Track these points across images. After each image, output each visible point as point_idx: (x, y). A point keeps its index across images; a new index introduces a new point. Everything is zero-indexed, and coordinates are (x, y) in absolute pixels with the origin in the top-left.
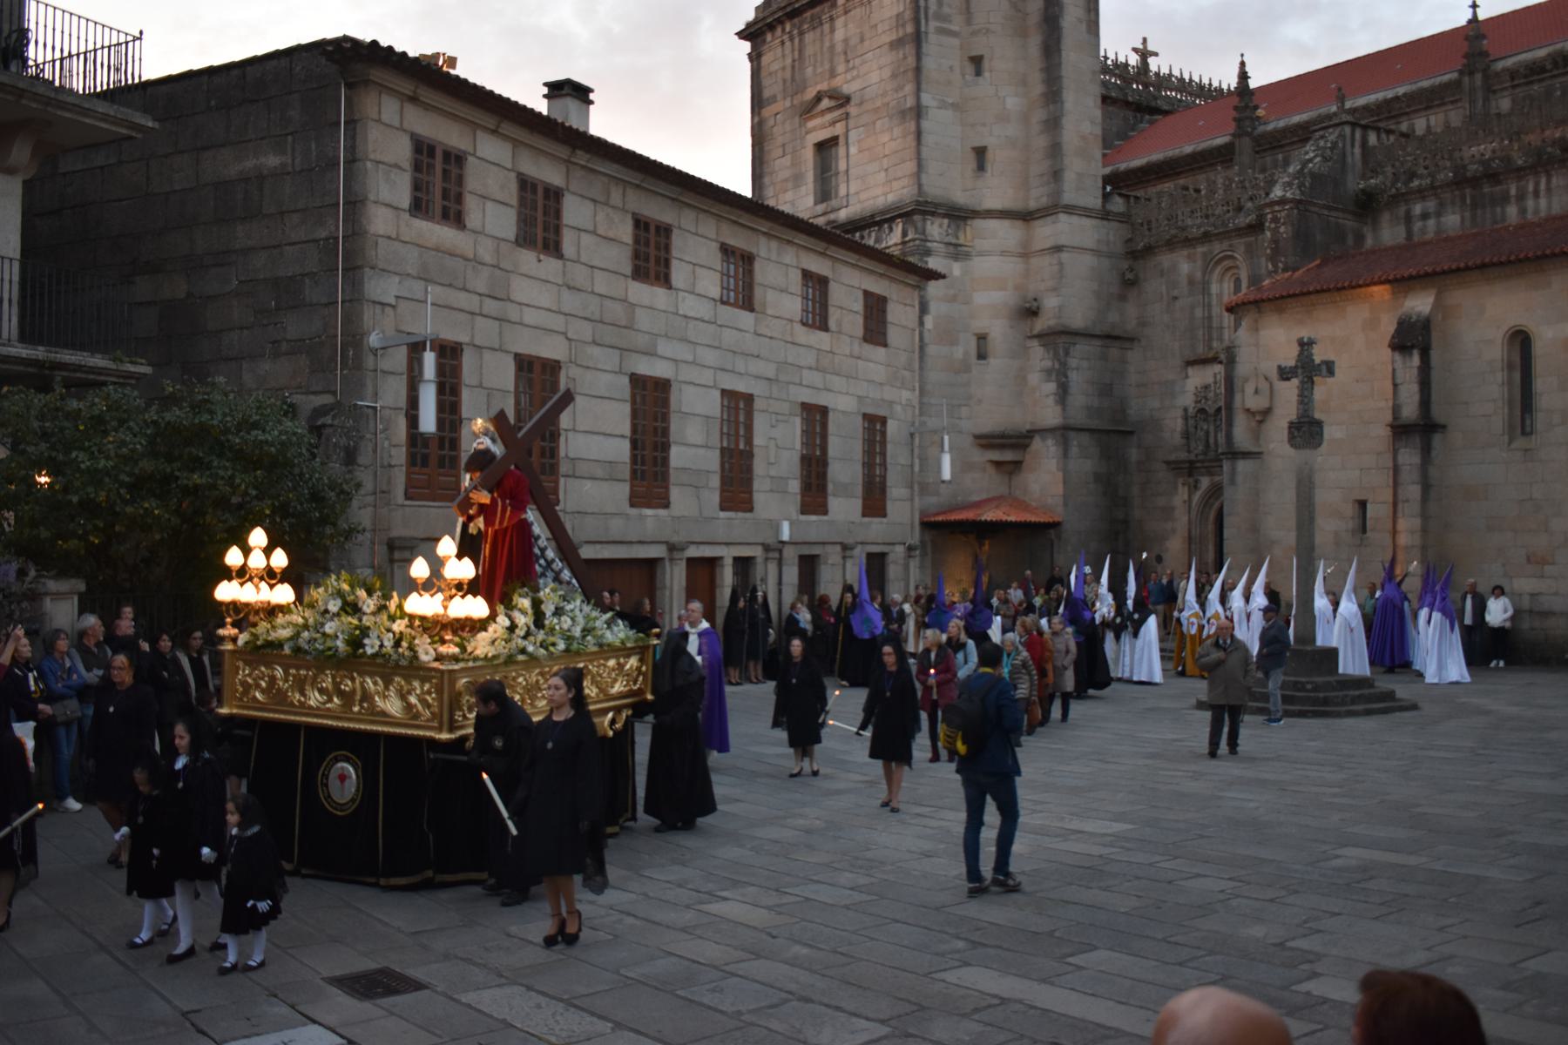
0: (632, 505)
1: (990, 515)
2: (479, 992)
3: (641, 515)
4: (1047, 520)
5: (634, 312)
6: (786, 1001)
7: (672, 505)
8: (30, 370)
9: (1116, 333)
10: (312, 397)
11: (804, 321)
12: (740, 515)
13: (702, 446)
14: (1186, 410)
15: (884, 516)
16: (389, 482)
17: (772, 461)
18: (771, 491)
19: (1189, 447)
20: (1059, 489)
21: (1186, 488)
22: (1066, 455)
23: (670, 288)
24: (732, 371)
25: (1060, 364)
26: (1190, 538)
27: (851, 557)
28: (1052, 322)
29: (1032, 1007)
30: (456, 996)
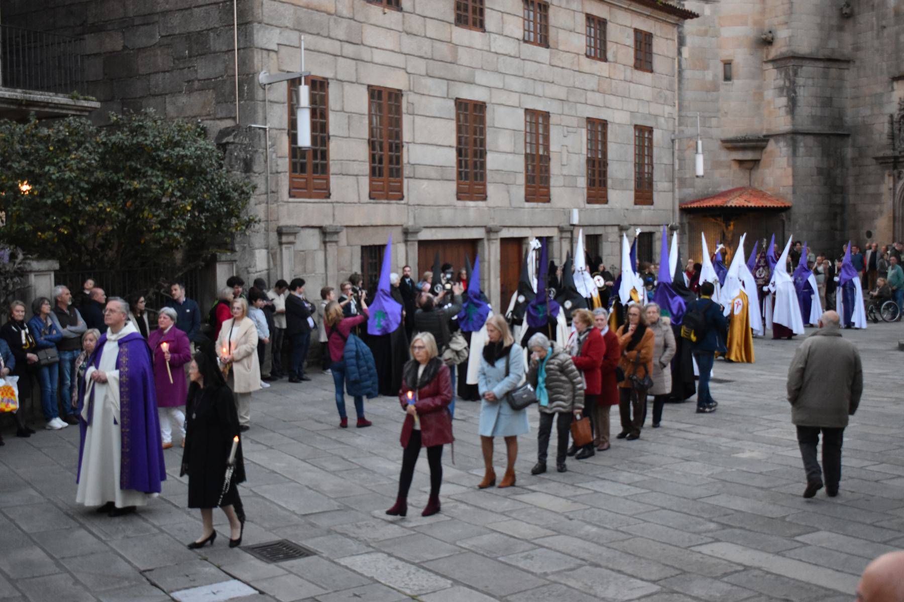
0: (459, 199)
2: (354, 557)
3: (465, 206)
4: (779, 205)
5: (456, 52)
6: (580, 566)
7: (488, 199)
8: (12, 107)
9: (837, 56)
10: (218, 122)
11: (588, 54)
12: (541, 204)
13: (511, 153)
15: (652, 203)
16: (277, 184)
17: (565, 162)
18: (564, 186)
19: (894, 145)
20: (790, 181)
21: (892, 178)
22: (794, 153)
23: (484, 31)
24: (533, 95)
25: (790, 82)
26: (894, 218)
28: (784, 50)
29: (768, 573)
30: (336, 560)
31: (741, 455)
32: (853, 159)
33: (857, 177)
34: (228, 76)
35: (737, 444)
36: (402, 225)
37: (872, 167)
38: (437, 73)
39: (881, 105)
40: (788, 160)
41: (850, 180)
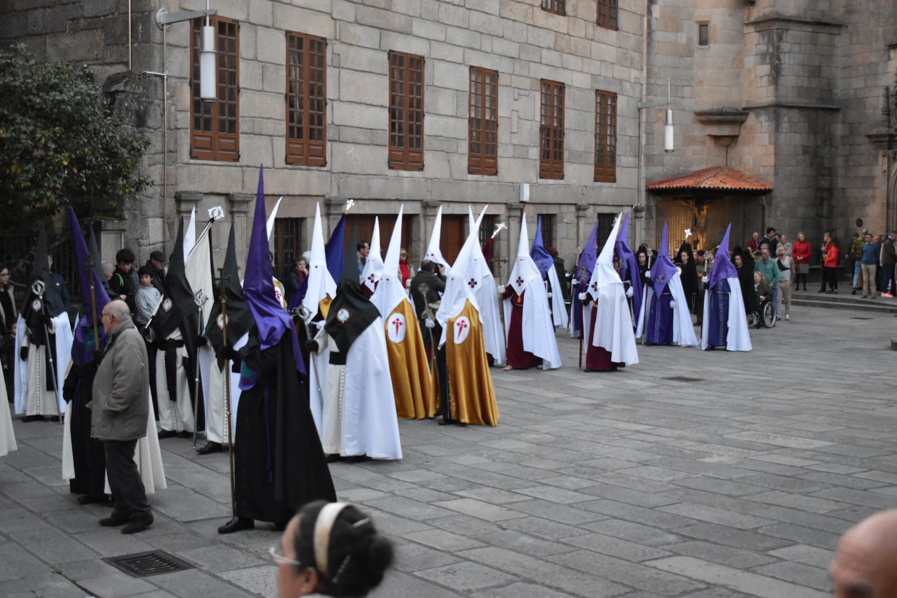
0: (391, 168)
1: (708, 183)
2: (239, 571)
3: (398, 176)
4: (759, 188)
6: (512, 582)
7: (425, 168)
10: (107, 68)
11: (544, 6)
12: (486, 177)
13: (452, 117)
14: (887, 89)
15: (614, 181)
16: (176, 142)
17: (515, 130)
18: (514, 157)
19: (889, 121)
20: (771, 161)
21: (886, 160)
22: (777, 129)
25: (774, 48)
26: (888, 204)
27: (584, 217)
28: (767, 11)
29: (735, 591)
30: (218, 574)
31: (707, 460)
32: (843, 137)
33: (847, 158)
34: (119, 14)
35: (704, 448)
36: (324, 196)
37: (865, 147)
38: (368, 21)
39: (876, 75)
40: (770, 137)
41: (840, 162)
